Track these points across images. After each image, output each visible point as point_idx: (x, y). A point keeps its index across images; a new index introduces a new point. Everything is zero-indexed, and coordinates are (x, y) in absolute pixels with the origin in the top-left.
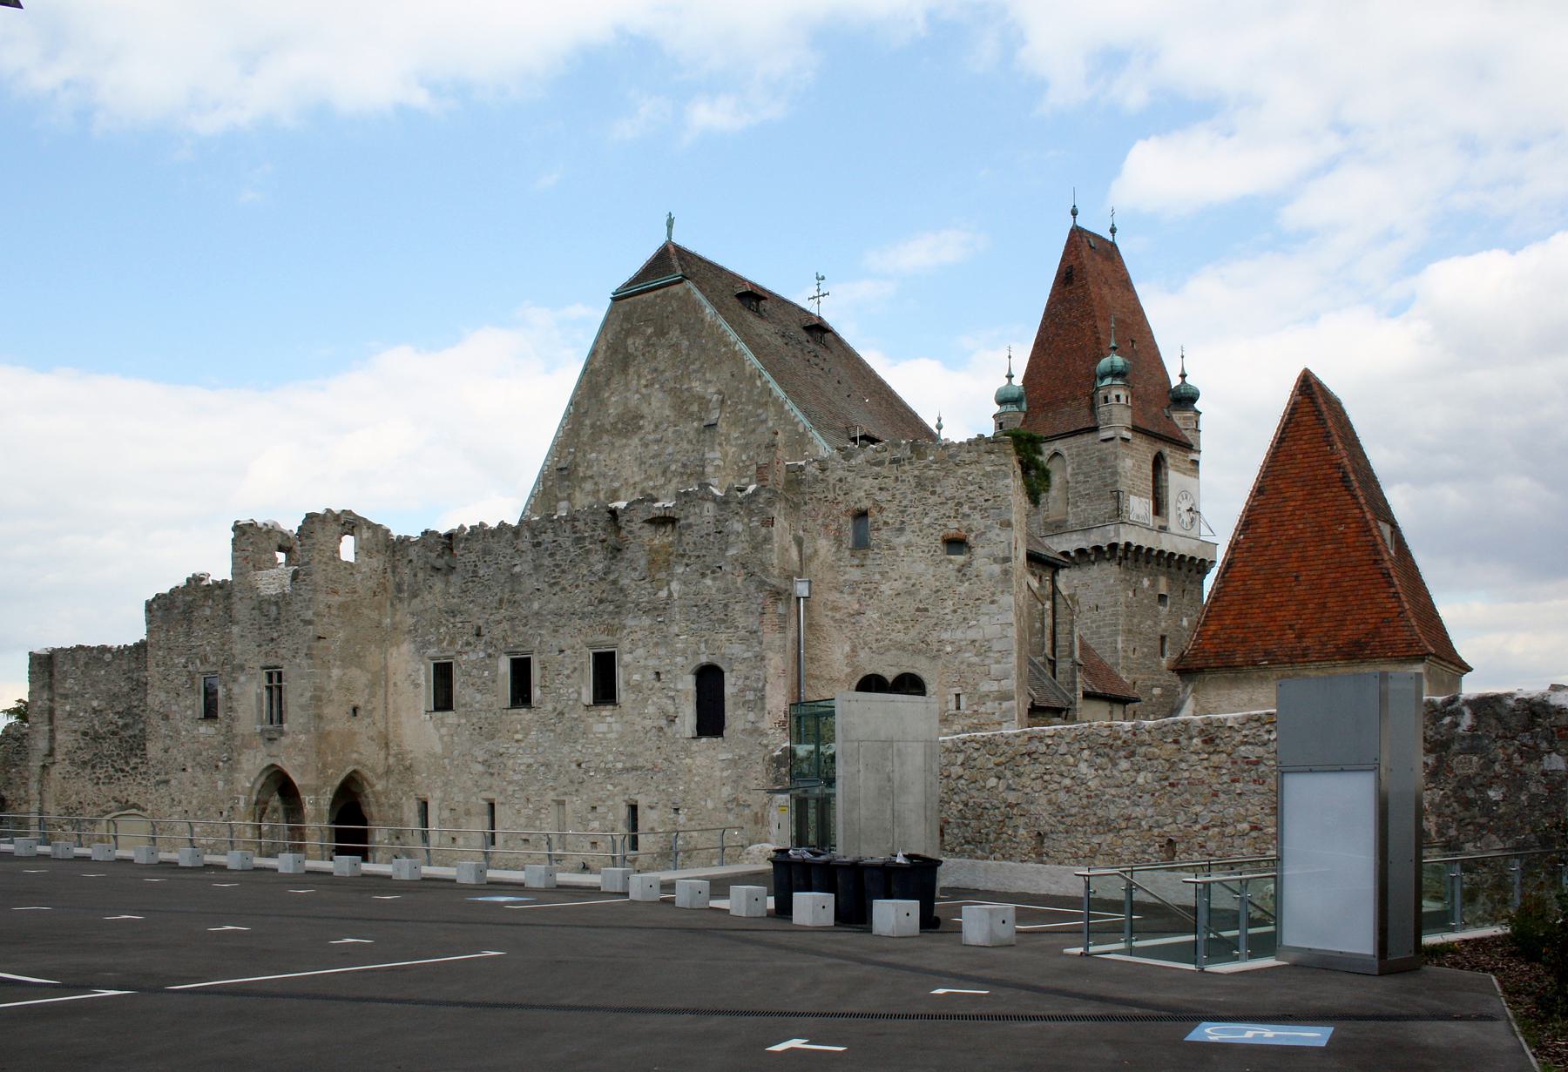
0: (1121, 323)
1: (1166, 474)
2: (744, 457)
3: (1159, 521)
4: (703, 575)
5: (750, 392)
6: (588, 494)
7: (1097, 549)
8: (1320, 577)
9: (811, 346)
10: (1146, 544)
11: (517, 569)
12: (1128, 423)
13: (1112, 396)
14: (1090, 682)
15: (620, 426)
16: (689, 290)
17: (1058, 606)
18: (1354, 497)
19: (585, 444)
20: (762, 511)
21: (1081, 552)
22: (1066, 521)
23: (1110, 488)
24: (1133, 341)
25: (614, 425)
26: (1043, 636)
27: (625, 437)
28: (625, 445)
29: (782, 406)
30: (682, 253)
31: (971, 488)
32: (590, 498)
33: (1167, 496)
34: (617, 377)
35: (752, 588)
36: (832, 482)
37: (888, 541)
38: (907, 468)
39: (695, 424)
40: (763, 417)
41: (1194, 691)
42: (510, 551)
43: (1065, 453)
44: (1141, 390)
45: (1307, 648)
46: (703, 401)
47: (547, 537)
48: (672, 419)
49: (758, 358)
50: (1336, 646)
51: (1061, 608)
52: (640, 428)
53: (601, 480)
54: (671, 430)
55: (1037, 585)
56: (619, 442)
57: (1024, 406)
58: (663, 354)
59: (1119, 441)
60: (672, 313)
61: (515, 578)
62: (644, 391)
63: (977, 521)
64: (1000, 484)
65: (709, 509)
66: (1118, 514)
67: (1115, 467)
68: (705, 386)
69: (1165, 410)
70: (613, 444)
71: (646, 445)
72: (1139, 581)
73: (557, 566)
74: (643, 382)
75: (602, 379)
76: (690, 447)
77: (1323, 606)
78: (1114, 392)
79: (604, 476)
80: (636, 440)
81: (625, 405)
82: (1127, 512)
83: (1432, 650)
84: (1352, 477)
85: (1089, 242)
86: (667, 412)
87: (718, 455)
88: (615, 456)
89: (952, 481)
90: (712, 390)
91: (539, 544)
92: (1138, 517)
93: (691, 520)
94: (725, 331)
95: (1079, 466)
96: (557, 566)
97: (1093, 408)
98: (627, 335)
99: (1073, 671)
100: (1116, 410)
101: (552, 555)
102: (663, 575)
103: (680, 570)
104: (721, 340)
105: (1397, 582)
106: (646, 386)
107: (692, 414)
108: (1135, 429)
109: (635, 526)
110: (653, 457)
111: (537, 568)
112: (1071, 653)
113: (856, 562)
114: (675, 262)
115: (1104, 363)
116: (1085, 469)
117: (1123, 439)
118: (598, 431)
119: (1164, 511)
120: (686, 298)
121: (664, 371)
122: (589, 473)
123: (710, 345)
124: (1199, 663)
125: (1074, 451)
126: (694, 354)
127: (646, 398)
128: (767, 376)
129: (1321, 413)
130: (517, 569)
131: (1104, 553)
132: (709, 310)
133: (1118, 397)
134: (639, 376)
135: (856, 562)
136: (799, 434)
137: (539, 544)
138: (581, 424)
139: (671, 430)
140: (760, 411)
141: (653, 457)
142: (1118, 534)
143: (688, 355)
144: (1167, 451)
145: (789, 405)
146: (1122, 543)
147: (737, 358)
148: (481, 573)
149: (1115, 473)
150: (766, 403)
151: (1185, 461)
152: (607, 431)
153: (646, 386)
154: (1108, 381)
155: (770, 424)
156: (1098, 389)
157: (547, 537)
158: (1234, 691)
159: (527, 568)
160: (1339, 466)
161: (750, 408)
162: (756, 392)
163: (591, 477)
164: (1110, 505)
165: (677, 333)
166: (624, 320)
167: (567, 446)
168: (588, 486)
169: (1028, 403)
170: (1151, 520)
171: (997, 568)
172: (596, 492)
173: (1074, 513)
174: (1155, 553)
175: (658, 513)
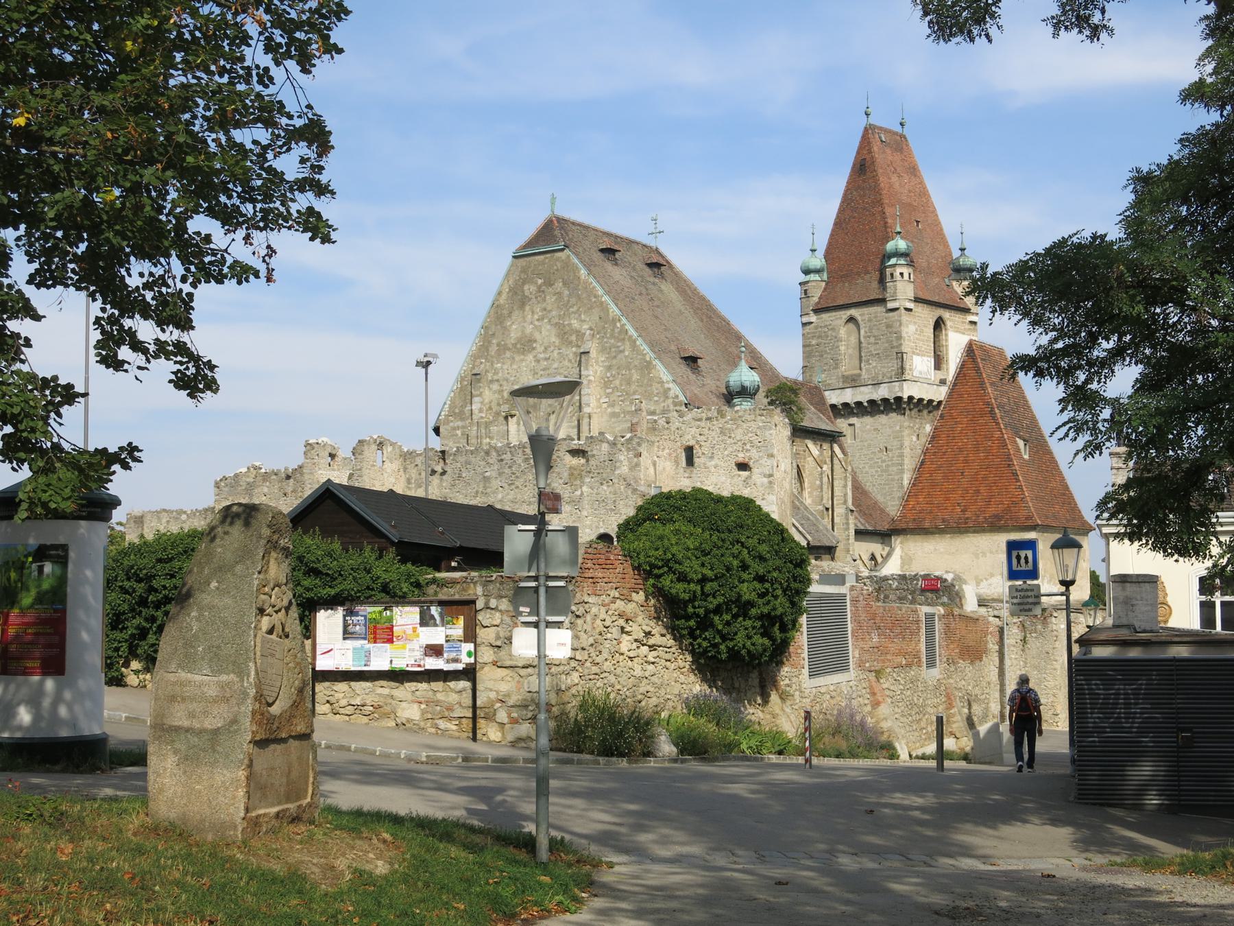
0: (909, 208)
1: (946, 335)
2: (608, 375)
3: (940, 375)
4: (602, 484)
5: (613, 330)
6: (495, 392)
7: (885, 400)
8: (977, 474)
9: (652, 279)
10: (926, 397)
11: (487, 474)
12: (911, 295)
13: (897, 274)
14: (863, 522)
15: (518, 346)
16: (569, 256)
17: (835, 466)
18: (998, 424)
19: (492, 357)
20: (635, 449)
21: (872, 402)
22: (860, 375)
23: (896, 350)
24: (918, 222)
25: (515, 345)
26: (822, 491)
27: (523, 354)
28: (522, 360)
29: (634, 341)
30: (561, 220)
31: (750, 435)
32: (496, 395)
33: (947, 354)
34: (517, 312)
35: (630, 492)
36: (673, 429)
37: (705, 464)
38: (715, 423)
39: (574, 349)
40: (622, 348)
41: (901, 543)
42: (482, 463)
43: (859, 318)
44: (925, 264)
45: (967, 518)
46: (580, 335)
47: (507, 457)
48: (557, 344)
49: (616, 305)
50: (985, 518)
51: (837, 466)
52: (534, 349)
53: (505, 383)
54: (556, 352)
55: (817, 453)
56: (517, 358)
57: (825, 277)
58: (551, 299)
59: (903, 311)
60: (557, 270)
61: (486, 479)
62: (536, 323)
63: (754, 453)
64: (767, 433)
65: (605, 447)
66: (901, 374)
67: (900, 332)
68: (582, 323)
69: (946, 280)
70: (513, 358)
71: (538, 361)
72: (922, 427)
73: (513, 474)
74: (536, 317)
75: (505, 312)
76: (570, 365)
77: (978, 491)
78: (898, 270)
79: (507, 380)
80: (530, 357)
81: (523, 331)
82: (910, 370)
83: (1040, 523)
84: (997, 411)
85: (880, 137)
86: (554, 340)
87: (591, 373)
88: (515, 367)
89: (740, 431)
90: (586, 326)
91: (502, 460)
92: (921, 373)
93: (595, 452)
94: (594, 287)
95: (871, 329)
96: (513, 474)
97: (882, 281)
98: (524, 284)
99: (847, 515)
100: (899, 285)
101: (510, 467)
102: (578, 482)
103: (587, 480)
104: (591, 293)
105: (1021, 478)
106: (538, 320)
107: (571, 342)
108: (917, 300)
109: (561, 454)
110: (544, 370)
111: (500, 474)
112: (845, 502)
113: (687, 475)
114: (557, 232)
115: (890, 246)
116: (875, 332)
117: (906, 309)
118: (503, 348)
119: (944, 366)
120: (567, 264)
121: (551, 311)
122: (496, 377)
123: (584, 296)
124: (904, 526)
125: (866, 317)
126: (573, 300)
127: (538, 328)
128: (624, 320)
129: (979, 368)
130: (487, 474)
131: (891, 404)
132: (583, 272)
133: (902, 274)
134: (533, 312)
135: (687, 475)
136: (646, 362)
137: (502, 460)
138: (490, 342)
139: (556, 352)
140: (619, 344)
141: (544, 370)
142: (902, 390)
143: (569, 301)
144: (946, 315)
145: (639, 342)
146: (905, 396)
147: (603, 307)
148: (464, 475)
149: (900, 338)
150: (624, 339)
151: (963, 322)
152: (509, 349)
153: (538, 320)
154: (893, 261)
155: (627, 353)
156: (886, 267)
157: (507, 457)
158: (925, 544)
159: (494, 474)
160: (988, 404)
161: (612, 341)
162: (616, 330)
163: (498, 381)
164: (894, 365)
165: (561, 284)
166: (521, 272)
167: (480, 357)
168: (495, 387)
169: (829, 273)
170: (934, 376)
171: (766, 480)
172: (501, 392)
173: (867, 370)
174: (935, 403)
175: (575, 447)
